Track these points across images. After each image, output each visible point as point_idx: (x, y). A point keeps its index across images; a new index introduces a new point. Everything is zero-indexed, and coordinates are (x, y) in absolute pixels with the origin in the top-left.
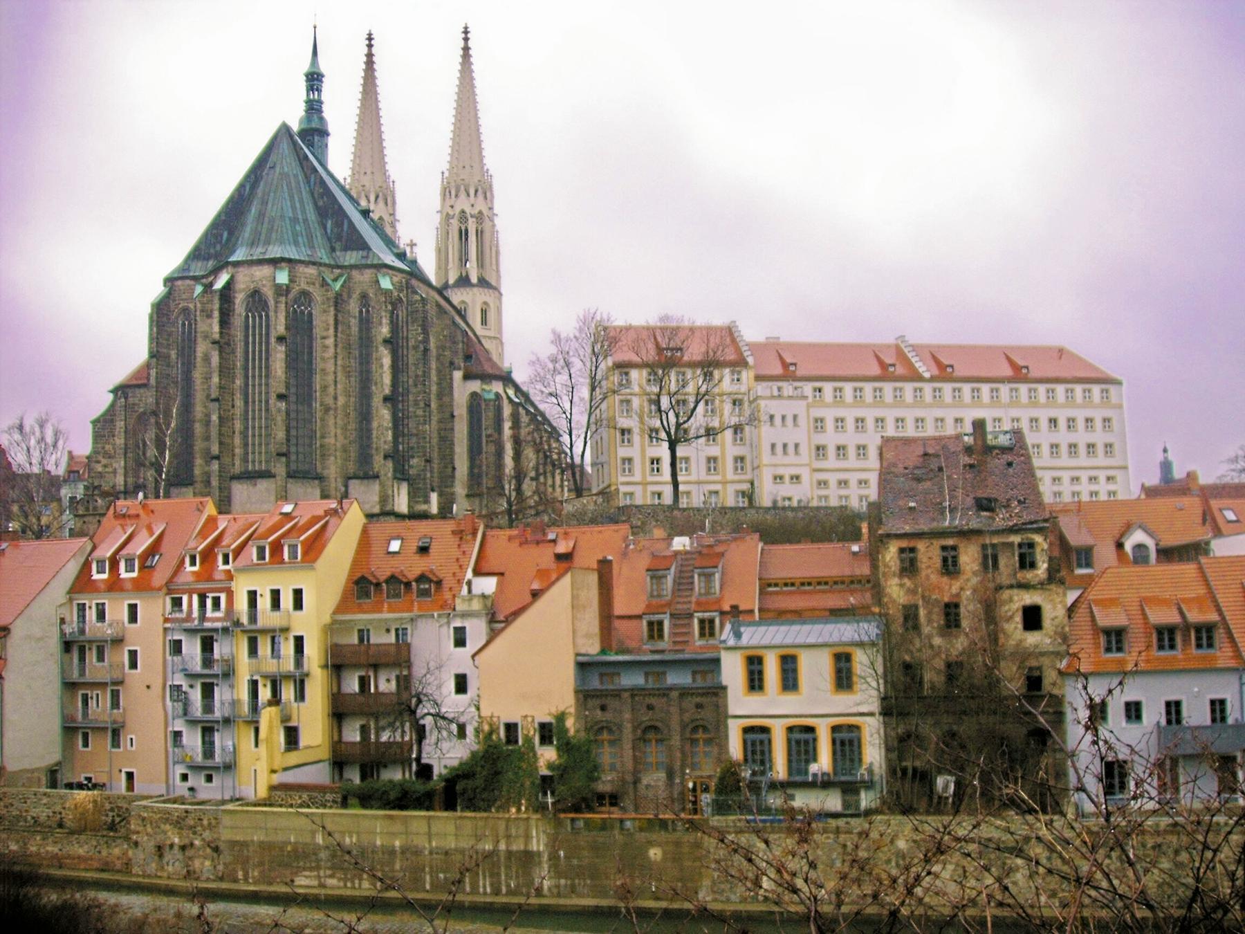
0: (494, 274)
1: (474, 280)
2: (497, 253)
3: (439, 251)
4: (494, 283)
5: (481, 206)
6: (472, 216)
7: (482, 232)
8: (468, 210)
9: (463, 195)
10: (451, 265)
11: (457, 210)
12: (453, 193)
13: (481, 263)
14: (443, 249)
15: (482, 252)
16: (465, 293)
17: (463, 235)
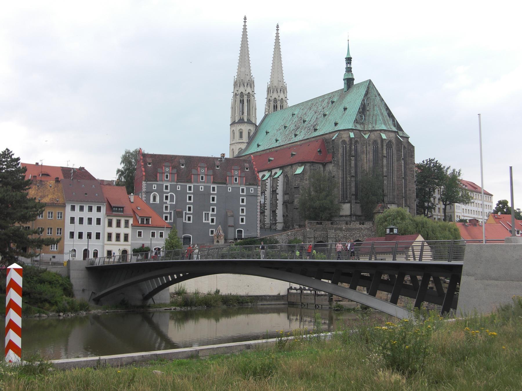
0: (254, 118)
1: (246, 120)
2: (255, 109)
3: (232, 108)
4: (254, 122)
5: (249, 90)
6: (246, 95)
7: (249, 101)
8: (244, 92)
9: (242, 87)
10: (237, 114)
11: (239, 92)
12: (238, 85)
13: (249, 114)
14: (234, 108)
15: (249, 109)
16: (242, 126)
17: (242, 102)
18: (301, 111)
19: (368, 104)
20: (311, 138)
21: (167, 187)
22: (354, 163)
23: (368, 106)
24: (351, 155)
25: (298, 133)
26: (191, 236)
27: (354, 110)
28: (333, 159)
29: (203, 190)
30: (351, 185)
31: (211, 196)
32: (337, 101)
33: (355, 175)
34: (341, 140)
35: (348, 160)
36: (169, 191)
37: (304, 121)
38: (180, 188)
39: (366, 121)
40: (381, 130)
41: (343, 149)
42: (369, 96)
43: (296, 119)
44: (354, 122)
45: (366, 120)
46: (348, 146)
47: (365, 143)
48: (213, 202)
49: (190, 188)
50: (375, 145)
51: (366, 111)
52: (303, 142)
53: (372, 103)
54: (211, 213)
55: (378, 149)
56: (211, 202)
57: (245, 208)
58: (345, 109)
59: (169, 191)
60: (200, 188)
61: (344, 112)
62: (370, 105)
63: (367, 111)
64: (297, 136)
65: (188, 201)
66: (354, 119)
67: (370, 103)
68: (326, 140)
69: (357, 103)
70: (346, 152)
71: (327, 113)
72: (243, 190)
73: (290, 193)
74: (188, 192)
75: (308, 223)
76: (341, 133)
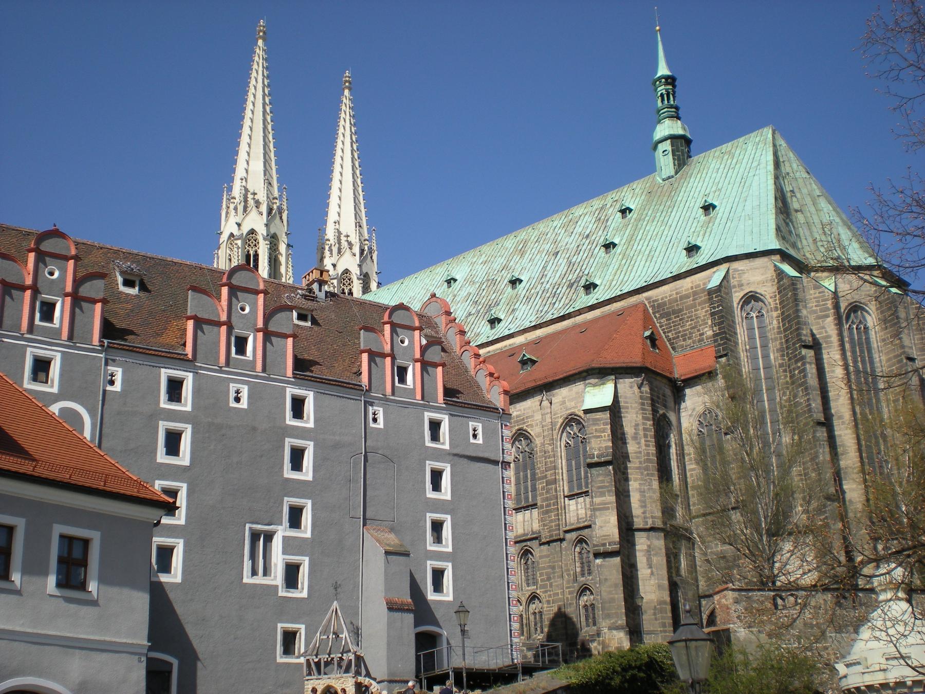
12: (240, 208)
18: (478, 267)
19: (792, 191)
20: (580, 312)
21: (41, 367)
22: (814, 371)
23: (794, 199)
24: (800, 340)
25: (502, 317)
26: (175, 662)
27: (756, 203)
28: (723, 360)
29: (244, 404)
30: (817, 457)
31: (289, 442)
32: (643, 208)
33: (826, 419)
34: (741, 294)
35: (781, 365)
36: (55, 390)
37: (515, 282)
38: (118, 379)
39: (804, 242)
40: (870, 268)
41: (751, 329)
42: (785, 168)
43: (472, 289)
44: (777, 235)
45: (803, 238)
46: (775, 314)
47: (828, 309)
48: (295, 475)
49: (175, 388)
50: (853, 323)
51: (793, 213)
52: (539, 333)
53: (805, 191)
54: (282, 532)
55: (868, 340)
56: (288, 473)
57: (449, 517)
58: (708, 208)
59: (55, 390)
60: (232, 395)
61: (703, 218)
62: (798, 195)
63: (797, 211)
64: (502, 324)
65: (161, 457)
66: (773, 226)
67: (796, 190)
68: (659, 307)
69: (755, 184)
70: (763, 336)
71: (616, 241)
72: (435, 426)
73: (547, 499)
74: (162, 405)
75: (737, 602)
76: (736, 270)
